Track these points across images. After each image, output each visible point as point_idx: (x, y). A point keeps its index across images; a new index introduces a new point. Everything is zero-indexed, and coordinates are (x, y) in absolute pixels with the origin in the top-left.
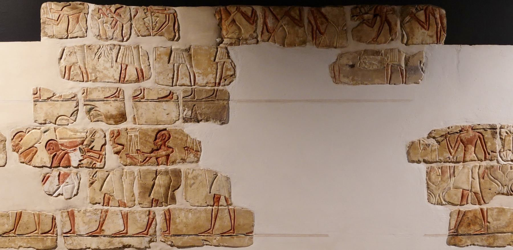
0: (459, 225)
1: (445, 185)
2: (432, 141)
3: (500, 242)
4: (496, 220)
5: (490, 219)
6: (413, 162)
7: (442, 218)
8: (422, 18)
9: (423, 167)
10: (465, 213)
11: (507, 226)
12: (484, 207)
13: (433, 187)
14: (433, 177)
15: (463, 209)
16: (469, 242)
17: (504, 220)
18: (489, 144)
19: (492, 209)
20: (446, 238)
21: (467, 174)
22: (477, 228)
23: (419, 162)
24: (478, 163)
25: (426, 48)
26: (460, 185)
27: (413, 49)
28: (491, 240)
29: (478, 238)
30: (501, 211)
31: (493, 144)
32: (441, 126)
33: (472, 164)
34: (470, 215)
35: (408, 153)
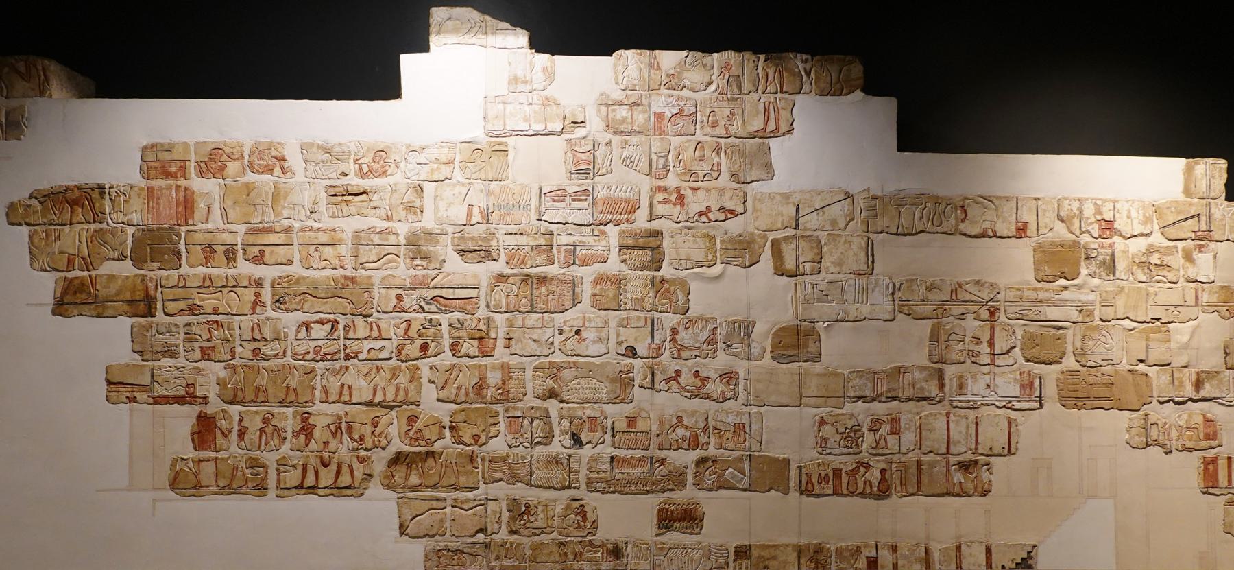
0: (65, 292)
1: (49, 249)
2: (34, 202)
3: (110, 312)
4: (105, 287)
5: (98, 287)
6: (13, 224)
7: (47, 285)
8: (22, 69)
9: (25, 230)
10: (71, 280)
11: (119, 293)
12: (93, 273)
13: (36, 251)
14: (36, 241)
15: (69, 275)
16: (76, 312)
17: (113, 289)
18: (97, 205)
19: (101, 276)
20: (50, 308)
21: (75, 237)
22: (84, 296)
23: (20, 225)
24: (86, 226)
25: (28, 101)
26: (65, 249)
27: (14, 103)
28: (100, 310)
29: (86, 307)
30: (111, 278)
31: (102, 205)
32: (45, 185)
33: (80, 226)
34: (76, 282)
35: (7, 215)
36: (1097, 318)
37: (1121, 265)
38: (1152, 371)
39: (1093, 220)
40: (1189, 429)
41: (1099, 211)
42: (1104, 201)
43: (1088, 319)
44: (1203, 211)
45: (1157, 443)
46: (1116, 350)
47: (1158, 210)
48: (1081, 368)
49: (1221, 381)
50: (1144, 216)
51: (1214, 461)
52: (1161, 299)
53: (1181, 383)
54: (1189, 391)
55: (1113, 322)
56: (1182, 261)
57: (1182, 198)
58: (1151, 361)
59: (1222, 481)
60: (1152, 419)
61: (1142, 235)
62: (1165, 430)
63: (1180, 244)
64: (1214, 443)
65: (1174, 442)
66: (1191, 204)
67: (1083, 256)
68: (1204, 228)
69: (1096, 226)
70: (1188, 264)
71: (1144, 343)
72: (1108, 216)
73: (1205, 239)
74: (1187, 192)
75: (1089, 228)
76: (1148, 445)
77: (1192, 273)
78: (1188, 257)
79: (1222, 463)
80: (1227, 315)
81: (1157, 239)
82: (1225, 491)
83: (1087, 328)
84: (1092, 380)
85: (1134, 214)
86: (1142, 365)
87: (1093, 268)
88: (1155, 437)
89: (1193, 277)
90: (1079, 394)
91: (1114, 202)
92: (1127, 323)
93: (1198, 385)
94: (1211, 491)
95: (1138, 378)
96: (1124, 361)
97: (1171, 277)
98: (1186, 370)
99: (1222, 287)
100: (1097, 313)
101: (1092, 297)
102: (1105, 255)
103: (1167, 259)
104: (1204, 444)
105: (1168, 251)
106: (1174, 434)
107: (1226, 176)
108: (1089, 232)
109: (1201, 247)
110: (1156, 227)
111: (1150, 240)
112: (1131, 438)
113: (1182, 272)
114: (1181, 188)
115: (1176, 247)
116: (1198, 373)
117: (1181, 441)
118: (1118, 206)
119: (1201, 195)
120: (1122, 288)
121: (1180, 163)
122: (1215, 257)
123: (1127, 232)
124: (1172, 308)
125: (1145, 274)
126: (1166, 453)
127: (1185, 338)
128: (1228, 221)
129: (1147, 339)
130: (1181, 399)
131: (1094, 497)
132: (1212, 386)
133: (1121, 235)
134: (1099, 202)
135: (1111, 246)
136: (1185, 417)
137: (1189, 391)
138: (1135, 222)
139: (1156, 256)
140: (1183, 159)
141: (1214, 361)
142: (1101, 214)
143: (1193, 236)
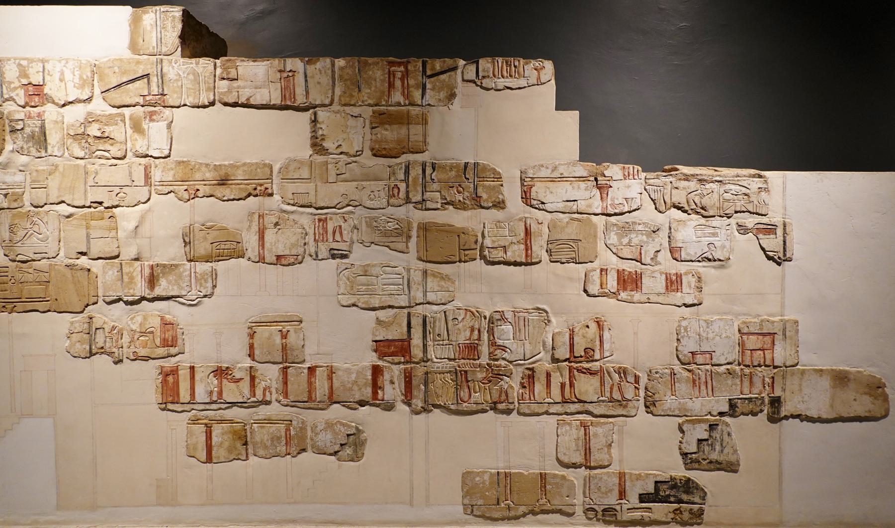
36: (27, 203)
37: (53, 139)
38: (97, 267)
39: (17, 84)
40: (143, 333)
41: (24, 74)
42: (30, 61)
43: (15, 205)
44: (152, 70)
45: (102, 351)
46: (52, 240)
47: (96, 70)
48: (11, 263)
49: (180, 276)
50: (81, 78)
51: (174, 371)
52: (102, 179)
53: (132, 278)
54: (140, 288)
55: (46, 208)
56: (130, 131)
57: (128, 54)
58: (94, 253)
59: (185, 395)
60: (97, 323)
61: (78, 101)
62: (117, 332)
63: (127, 111)
64: (173, 351)
65: (125, 349)
66: (138, 62)
67: (8, 129)
68: (155, 90)
69: (21, 92)
70: (136, 136)
71: (84, 232)
72: (36, 79)
73: (157, 103)
74: (134, 47)
75: (13, 95)
76: (92, 354)
77: (141, 145)
78: (137, 127)
79: (184, 374)
80: (186, 196)
81: (99, 106)
82: (188, 407)
83: (14, 215)
84: (19, 276)
85: (68, 76)
86: (84, 258)
87: (20, 143)
88: (101, 344)
89: (142, 150)
90: (7, 294)
91: (43, 61)
92: (64, 209)
93: (152, 281)
94: (170, 406)
95: (79, 273)
96: (62, 254)
97: (115, 151)
98: (137, 263)
99: (179, 163)
100: (26, 197)
101: (19, 177)
102: (32, 126)
103: (108, 130)
104: (162, 351)
105: (110, 120)
106: (126, 339)
107: (179, 26)
108: (14, 100)
109: (152, 114)
110: (97, 91)
111: (90, 107)
112: (72, 345)
113: (129, 145)
114: (126, 41)
115: (124, 115)
116: (152, 267)
117: (133, 349)
118: (46, 64)
119: (151, 50)
120: (57, 166)
121: (128, 9)
122: (169, 126)
123: (61, 98)
124: (117, 190)
125: (83, 148)
126: (116, 363)
127: (131, 225)
128: (185, 81)
129: (87, 228)
130: (130, 299)
131: (31, 415)
132: (169, 282)
133: (53, 102)
134: (24, 63)
135: (39, 115)
136: (139, 319)
137: (140, 288)
138: (70, 85)
139: (95, 126)
140: (129, 7)
141: (170, 252)
142: (26, 76)
143: (141, 101)
